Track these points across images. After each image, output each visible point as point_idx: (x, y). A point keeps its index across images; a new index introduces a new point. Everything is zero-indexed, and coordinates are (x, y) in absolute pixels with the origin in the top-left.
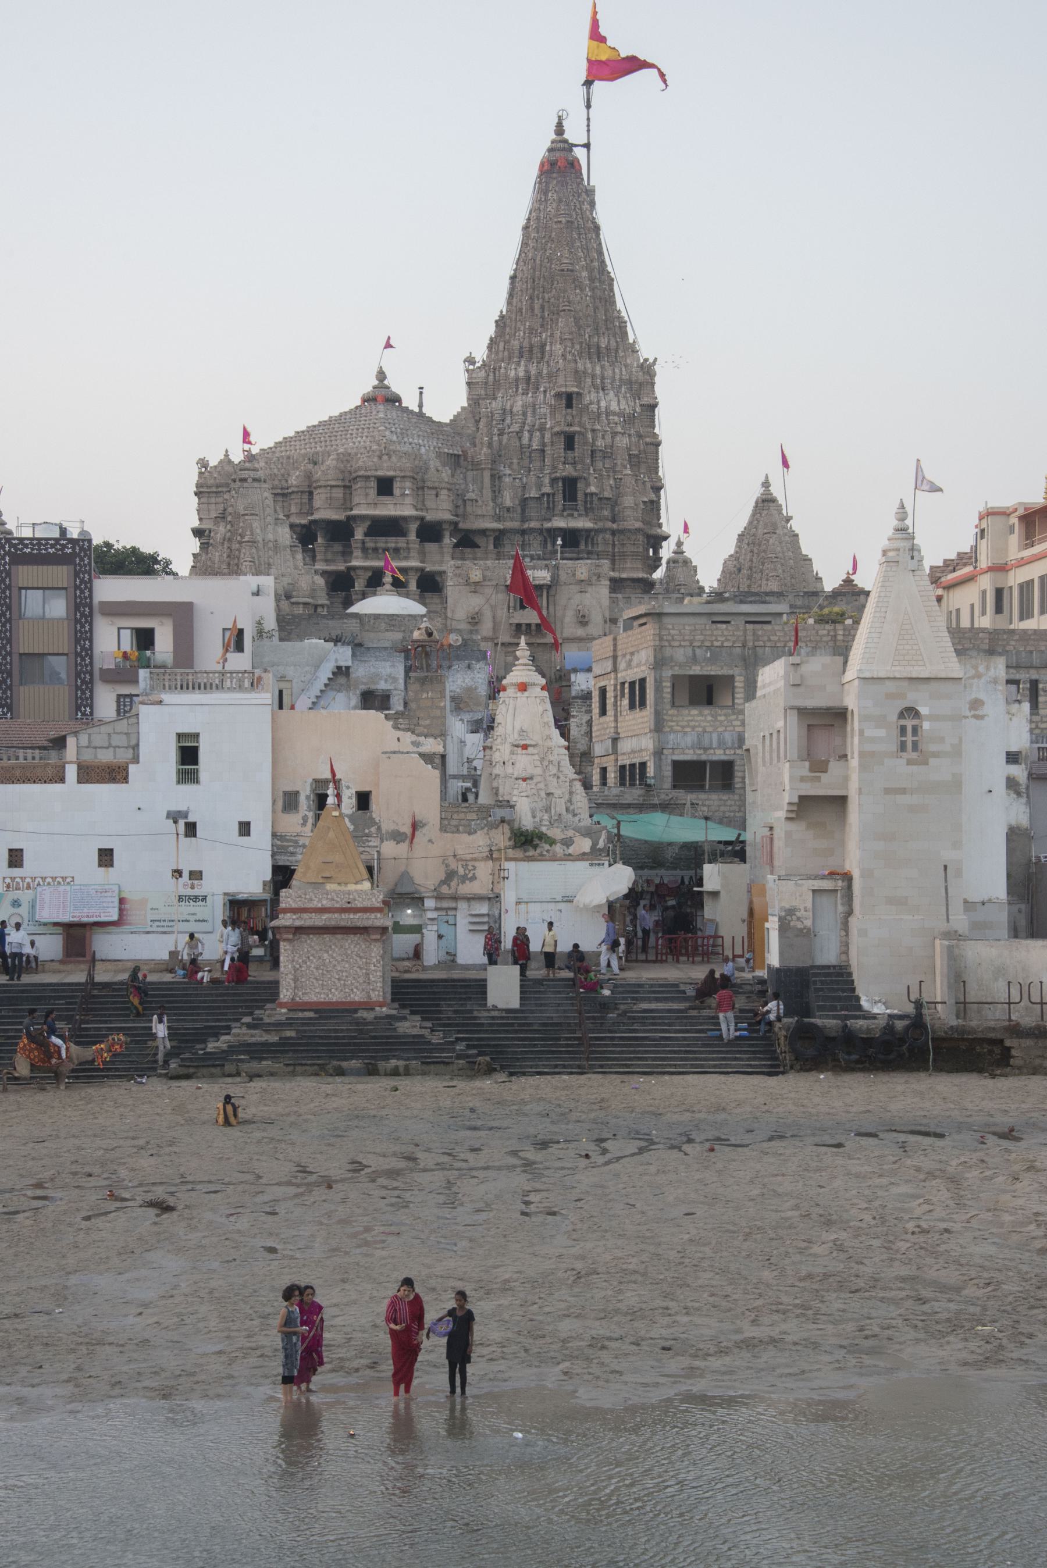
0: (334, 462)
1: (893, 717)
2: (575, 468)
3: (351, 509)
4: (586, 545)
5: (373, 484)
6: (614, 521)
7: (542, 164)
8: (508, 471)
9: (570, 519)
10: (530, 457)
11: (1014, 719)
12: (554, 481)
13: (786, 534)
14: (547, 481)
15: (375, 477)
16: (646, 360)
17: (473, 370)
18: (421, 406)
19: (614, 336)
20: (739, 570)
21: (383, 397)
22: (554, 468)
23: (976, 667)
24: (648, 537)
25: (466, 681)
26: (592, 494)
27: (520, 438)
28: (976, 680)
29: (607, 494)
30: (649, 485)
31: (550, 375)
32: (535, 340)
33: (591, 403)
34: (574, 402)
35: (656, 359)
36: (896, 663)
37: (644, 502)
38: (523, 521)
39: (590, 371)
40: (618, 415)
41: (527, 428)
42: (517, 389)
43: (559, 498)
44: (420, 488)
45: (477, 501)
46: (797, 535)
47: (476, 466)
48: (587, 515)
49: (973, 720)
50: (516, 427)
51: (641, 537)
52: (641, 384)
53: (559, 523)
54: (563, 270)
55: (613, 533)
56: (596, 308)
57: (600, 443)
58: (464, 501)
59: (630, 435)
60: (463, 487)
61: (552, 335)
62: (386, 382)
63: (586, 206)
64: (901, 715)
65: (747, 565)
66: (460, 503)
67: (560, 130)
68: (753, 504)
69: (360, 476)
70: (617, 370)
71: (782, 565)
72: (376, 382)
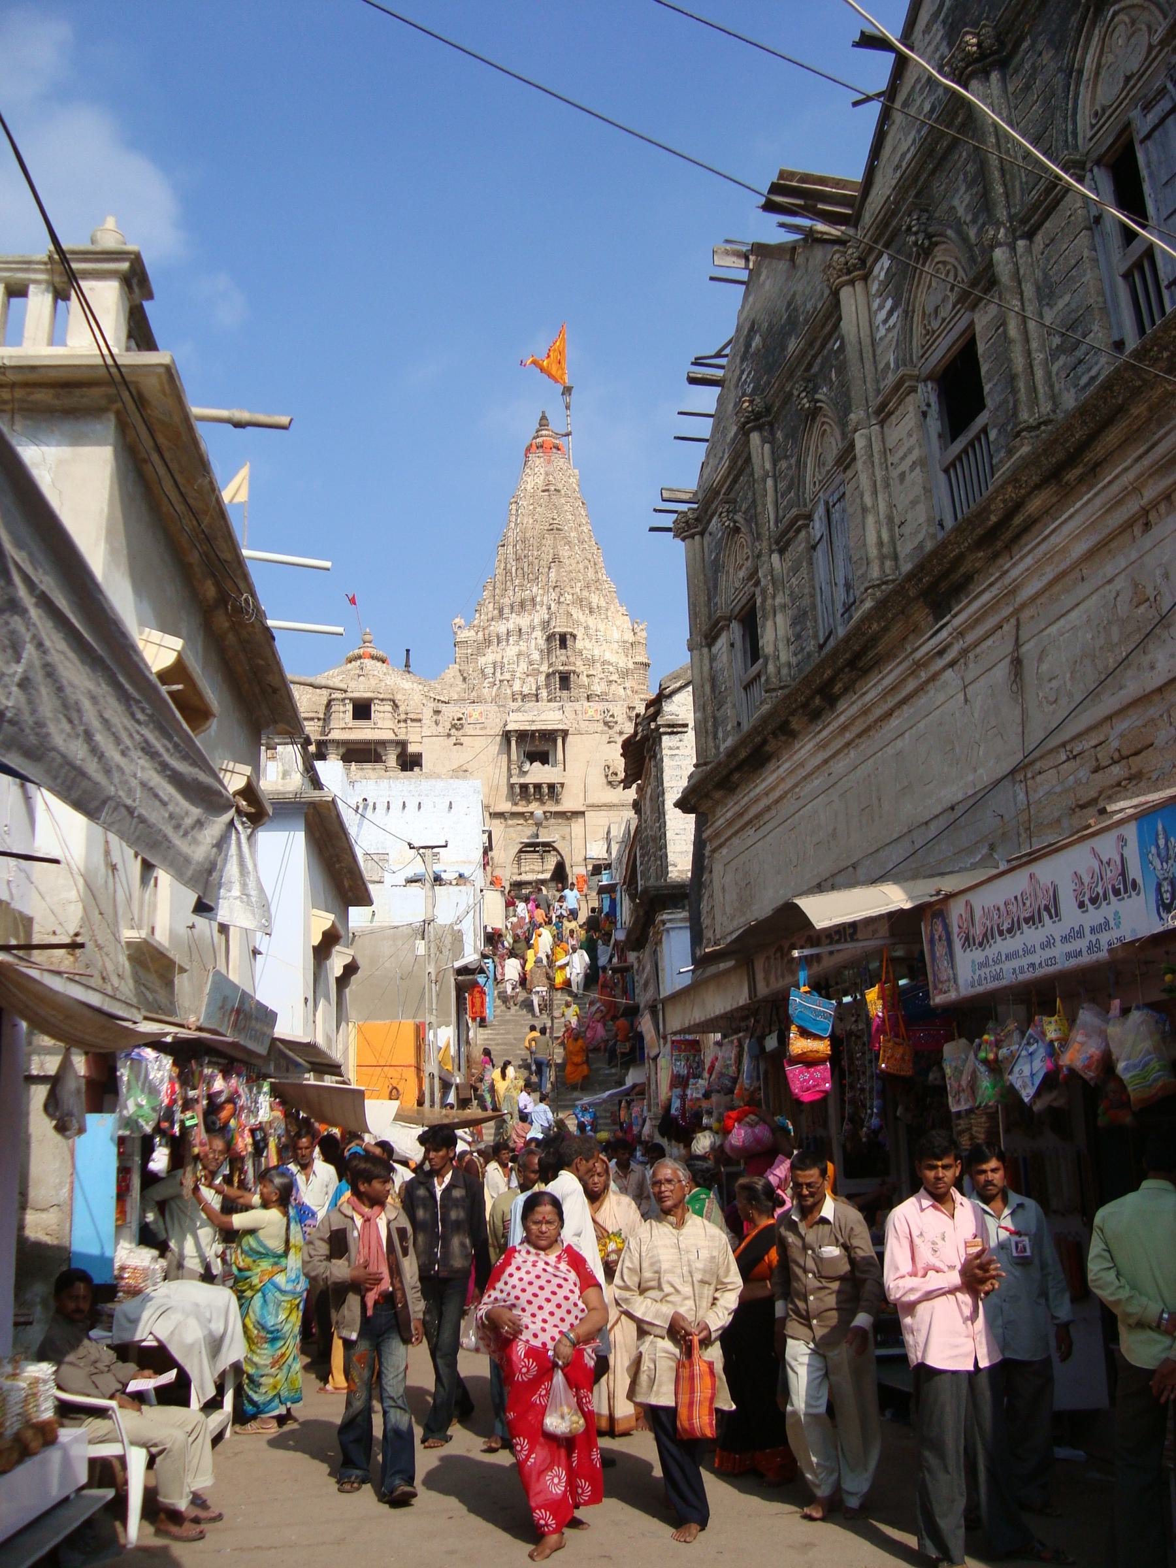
5: (350, 707)
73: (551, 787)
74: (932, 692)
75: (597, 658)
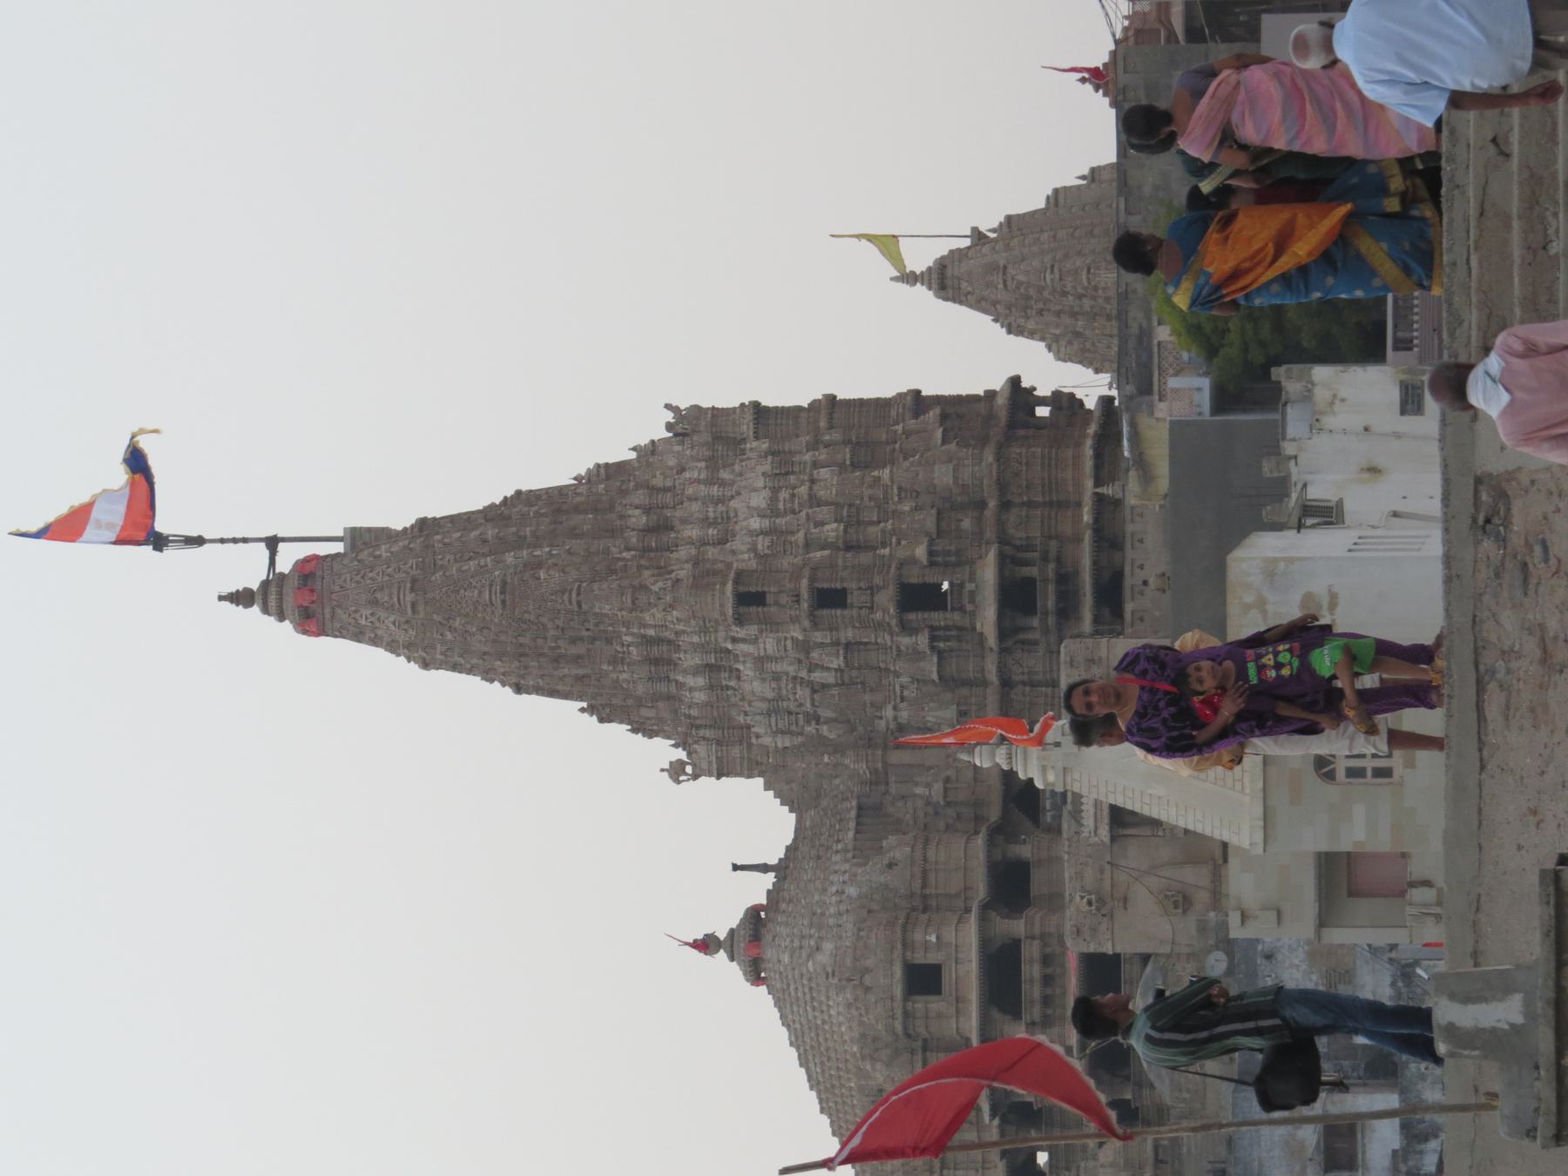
0: (879, 1066)
1: (1331, 791)
2: (880, 588)
3: (968, 1040)
4: (1027, 563)
5: (920, 1003)
6: (981, 505)
7: (306, 632)
8: (889, 712)
9: (978, 599)
10: (859, 668)
11: (1342, 393)
12: (906, 628)
13: (1007, 248)
14: (905, 641)
16: (669, 427)
17: (694, 766)
18: (764, 868)
19: (623, 493)
20: (1078, 335)
21: (751, 944)
22: (879, 626)
23: (1247, 608)
24: (1012, 425)
25: (1296, 962)
26: (931, 553)
27: (824, 686)
28: (1270, 608)
29: (929, 520)
30: (912, 423)
31: (704, 630)
33: (754, 549)
34: (753, 589)
35: (668, 407)
36: (1238, 786)
37: (944, 442)
38: (985, 683)
39: (693, 552)
40: (775, 491)
41: (803, 674)
42: (728, 688)
43: (937, 618)
44: (924, 904)
45: (947, 780)
46: (1009, 218)
47: (879, 778)
48: (972, 562)
49: (1339, 610)
50: (803, 693)
51: (1015, 450)
52: (718, 438)
53: (988, 618)
54: (503, 602)
55: (1005, 505)
56: (574, 534)
57: (832, 530)
58: (948, 804)
59: (816, 465)
60: (920, 803)
61: (627, 624)
62: (722, 935)
63: (383, 551)
64: (1330, 776)
65: (1067, 320)
66: (951, 812)
67: (242, 598)
68: (949, 304)
69: (905, 1028)
70: (690, 491)
71: (1066, 256)
72: (722, 955)
75: (766, 523)
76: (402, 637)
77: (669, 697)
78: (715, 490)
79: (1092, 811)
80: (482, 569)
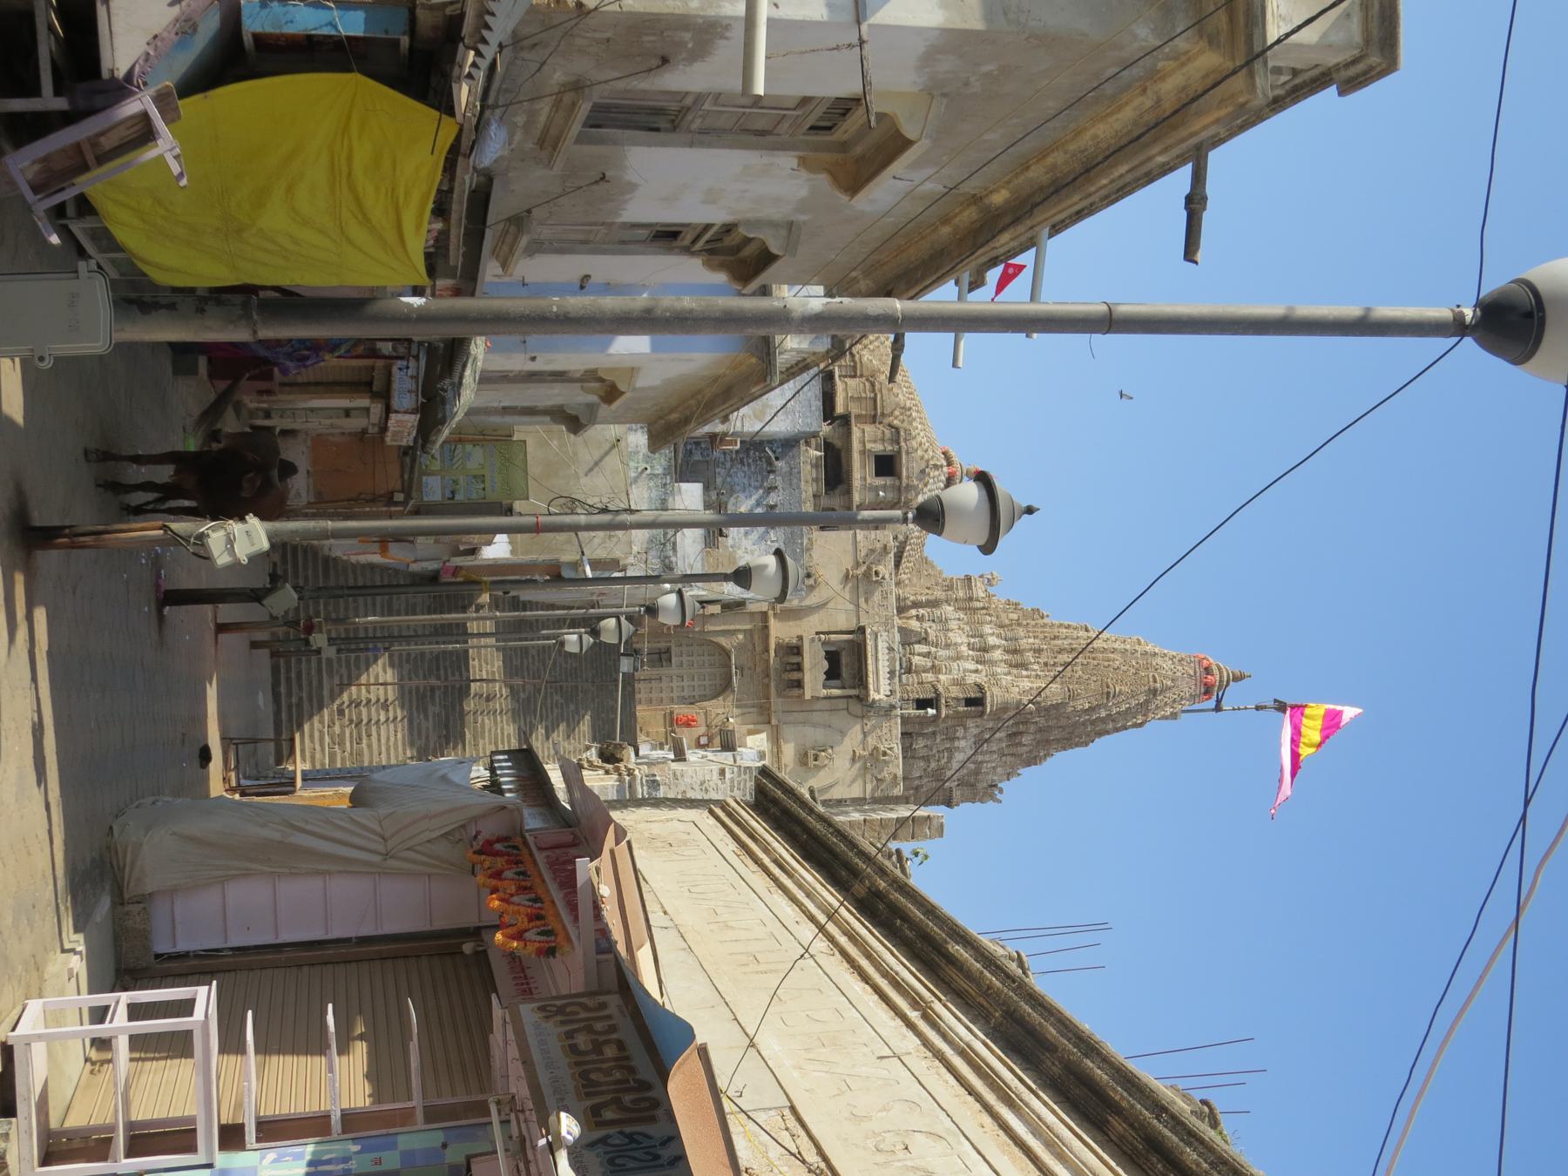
15: (899, 452)
16: (1001, 791)
32: (1029, 656)
33: (965, 729)
57: (920, 743)
73: (799, 684)
74: (893, 1024)
76: (1159, 660)
77: (1001, 626)
78: (980, 758)
79: (880, 655)
80: (1117, 705)
